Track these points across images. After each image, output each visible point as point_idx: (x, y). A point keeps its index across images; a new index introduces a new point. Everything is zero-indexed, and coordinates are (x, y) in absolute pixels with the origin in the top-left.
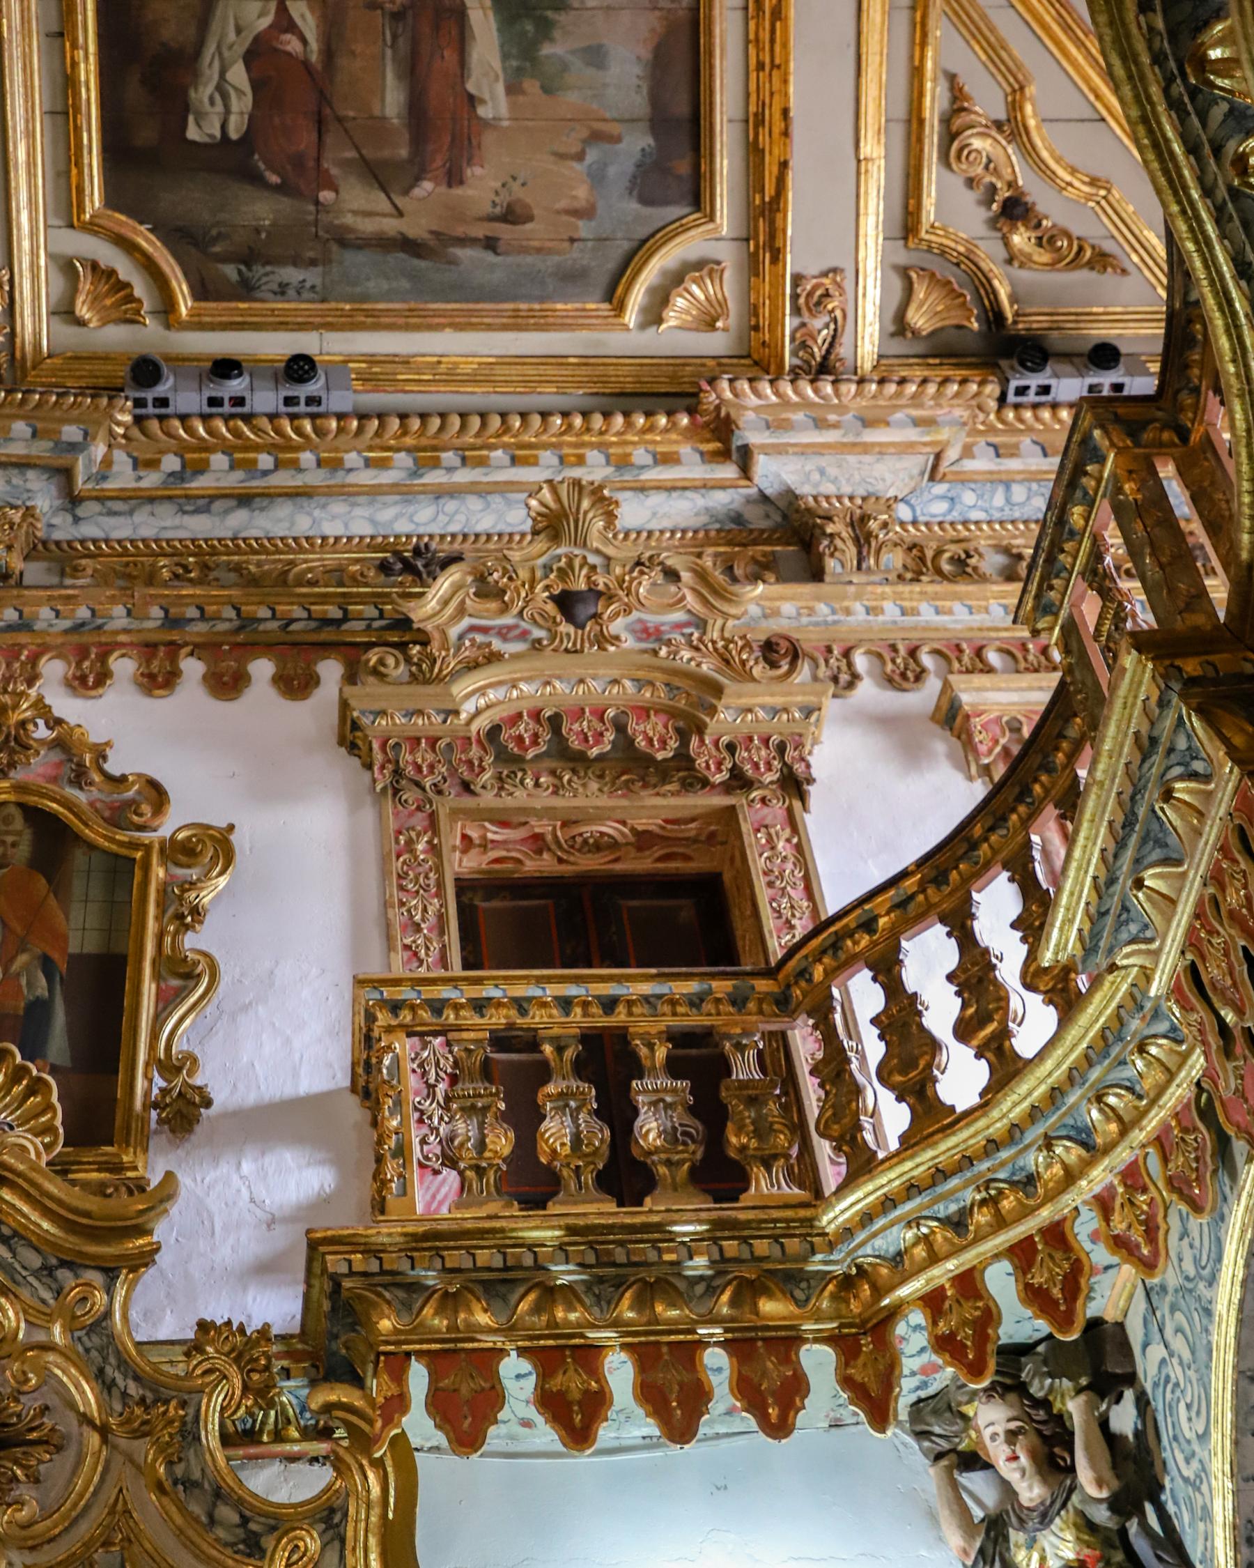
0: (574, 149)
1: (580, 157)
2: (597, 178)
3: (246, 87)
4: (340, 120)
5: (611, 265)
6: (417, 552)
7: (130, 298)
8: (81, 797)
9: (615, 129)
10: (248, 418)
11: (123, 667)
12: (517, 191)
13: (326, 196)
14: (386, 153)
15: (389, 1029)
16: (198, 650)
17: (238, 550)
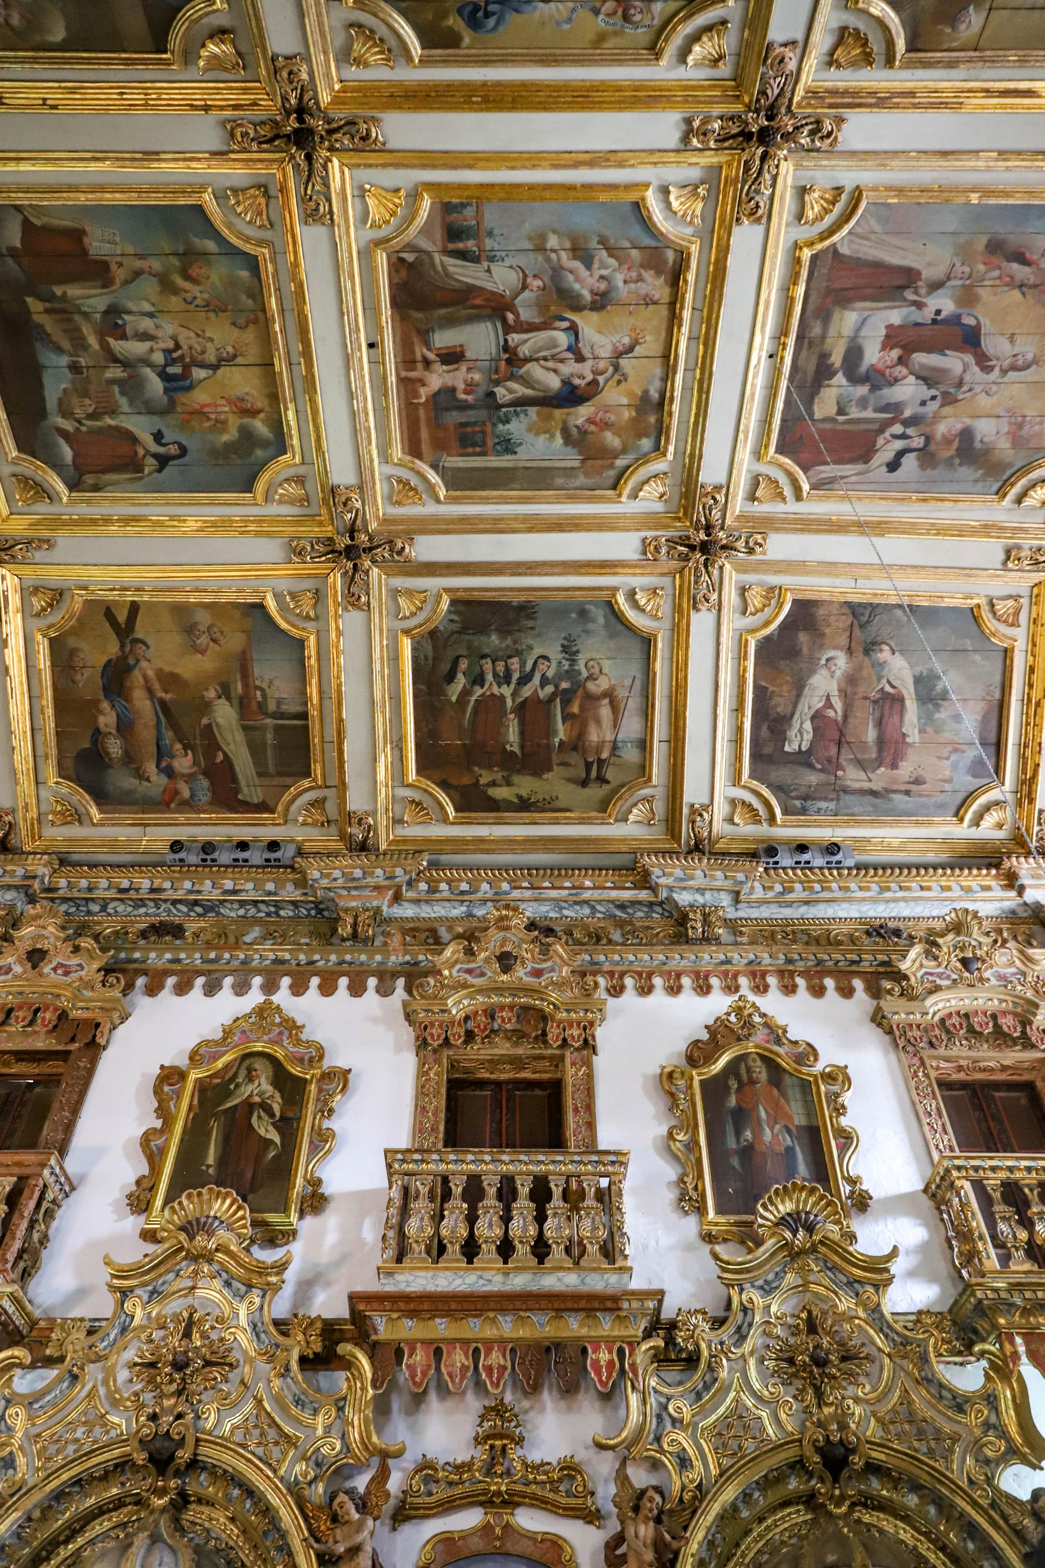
0: (946, 755)
1: (948, 758)
2: (954, 767)
3: (811, 731)
4: (848, 743)
5: (958, 802)
6: (881, 927)
7: (757, 815)
8: (780, 1050)
9: (964, 747)
10: (811, 869)
11: (772, 980)
12: (921, 772)
13: (840, 773)
14: (866, 756)
15: (959, 1178)
16: (801, 974)
17: (804, 924)
